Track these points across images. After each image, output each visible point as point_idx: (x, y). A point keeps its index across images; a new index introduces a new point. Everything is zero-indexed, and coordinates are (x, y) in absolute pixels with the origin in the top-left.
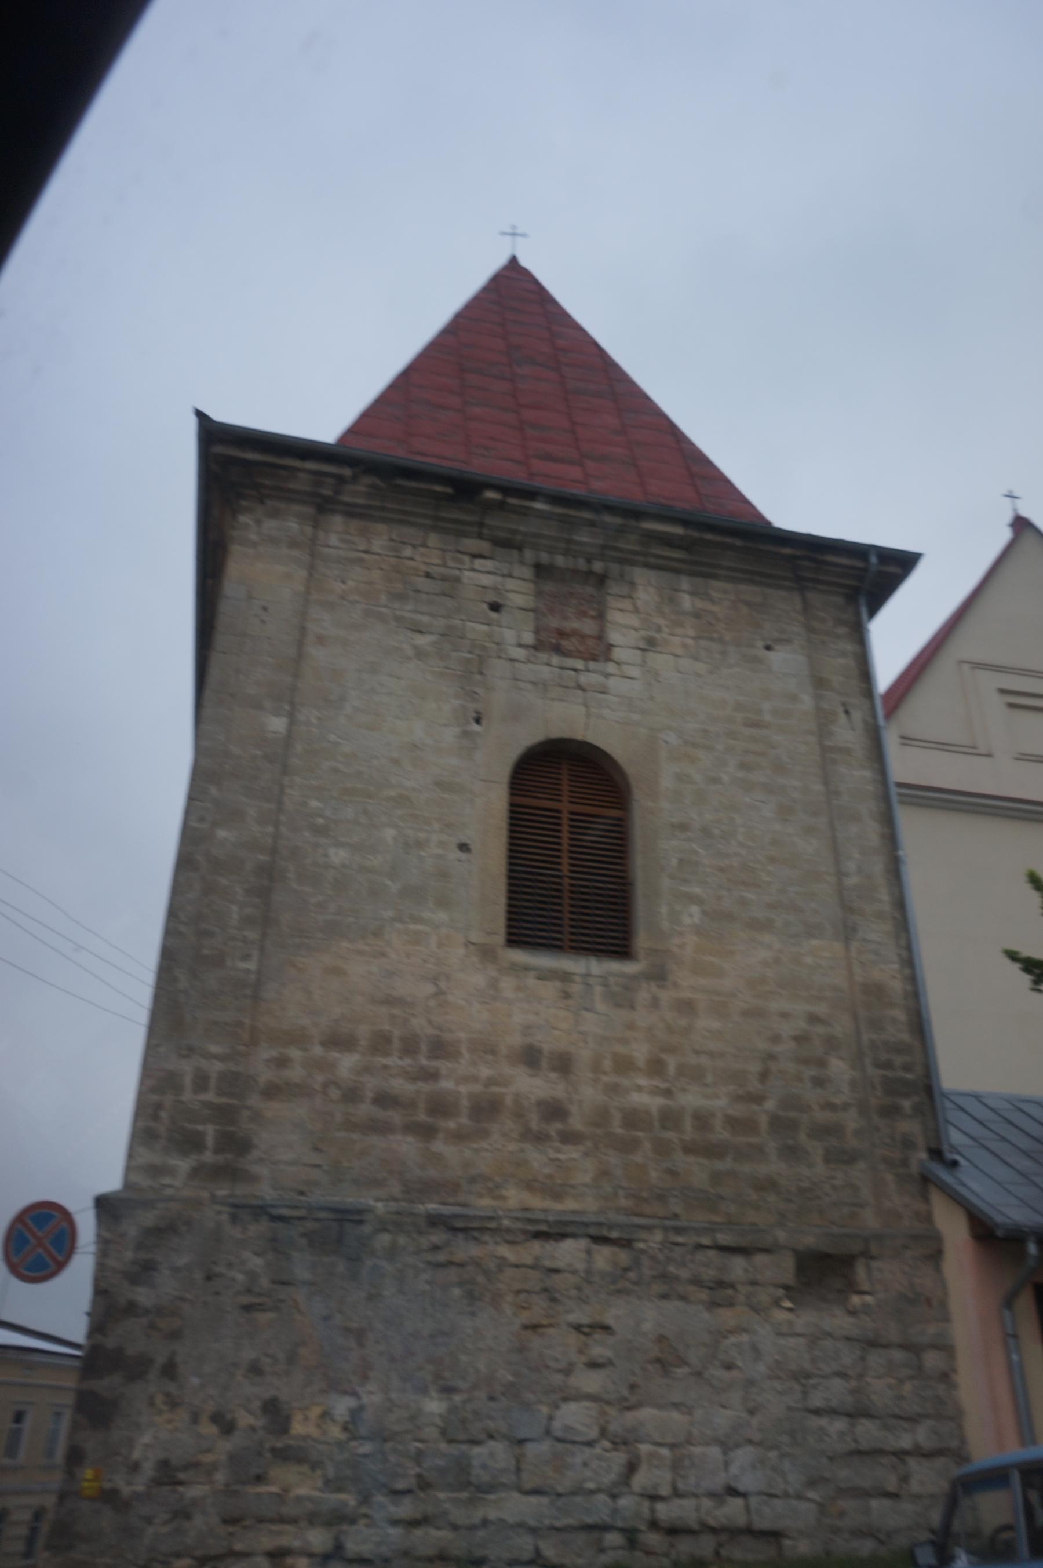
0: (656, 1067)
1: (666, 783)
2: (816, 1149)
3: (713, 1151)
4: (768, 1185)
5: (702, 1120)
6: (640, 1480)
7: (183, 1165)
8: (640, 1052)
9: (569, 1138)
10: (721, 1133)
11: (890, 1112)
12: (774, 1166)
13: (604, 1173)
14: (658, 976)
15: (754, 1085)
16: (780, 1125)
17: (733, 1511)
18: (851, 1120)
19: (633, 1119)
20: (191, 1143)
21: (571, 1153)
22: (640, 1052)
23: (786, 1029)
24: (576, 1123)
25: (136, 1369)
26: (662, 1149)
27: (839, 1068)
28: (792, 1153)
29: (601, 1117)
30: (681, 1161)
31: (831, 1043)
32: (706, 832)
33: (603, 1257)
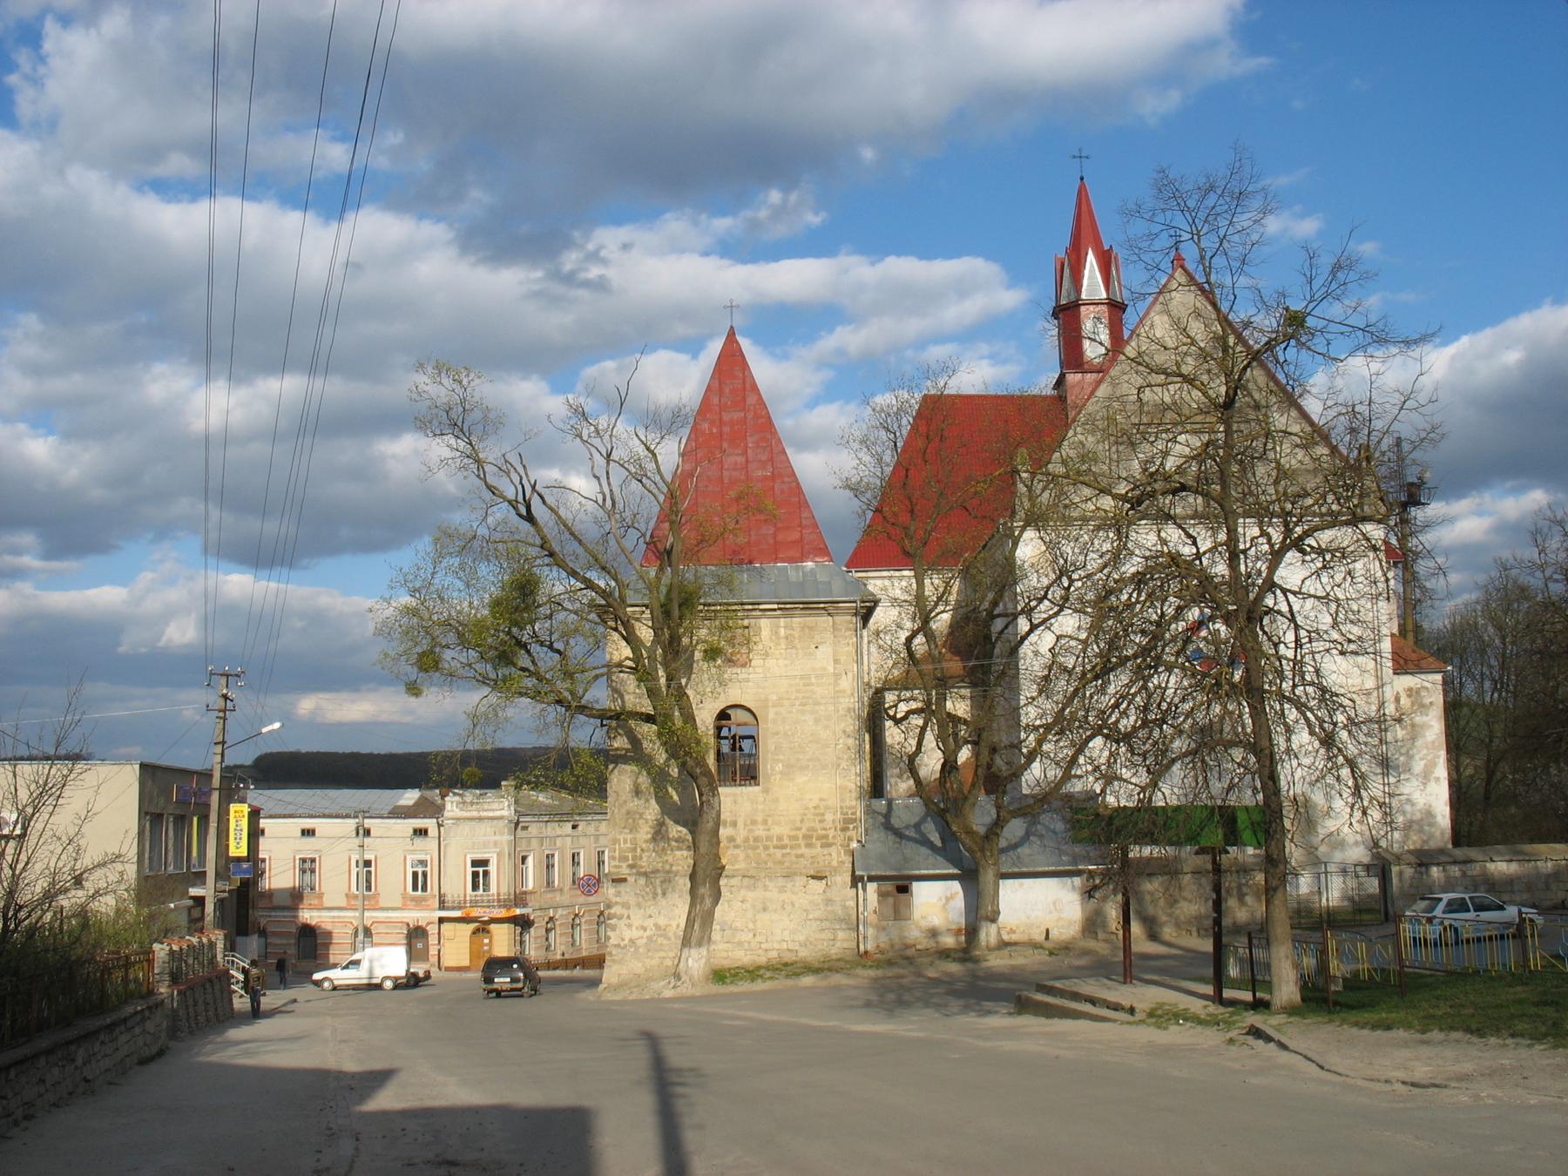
0: (765, 822)
1: (771, 715)
2: (819, 844)
3: (784, 847)
4: (802, 856)
5: (780, 838)
6: (758, 939)
7: (624, 865)
8: (760, 819)
9: (737, 847)
10: (786, 841)
11: (844, 829)
12: (803, 850)
13: (748, 856)
14: (766, 791)
15: (798, 824)
16: (805, 837)
17: (785, 946)
18: (831, 833)
19: (756, 839)
20: (625, 859)
21: (736, 851)
22: (760, 819)
23: (811, 805)
24: (739, 841)
25: (620, 918)
26: (766, 848)
27: (829, 817)
28: (809, 845)
29: (746, 840)
30: (772, 850)
31: (827, 808)
32: (785, 734)
33: (746, 880)
